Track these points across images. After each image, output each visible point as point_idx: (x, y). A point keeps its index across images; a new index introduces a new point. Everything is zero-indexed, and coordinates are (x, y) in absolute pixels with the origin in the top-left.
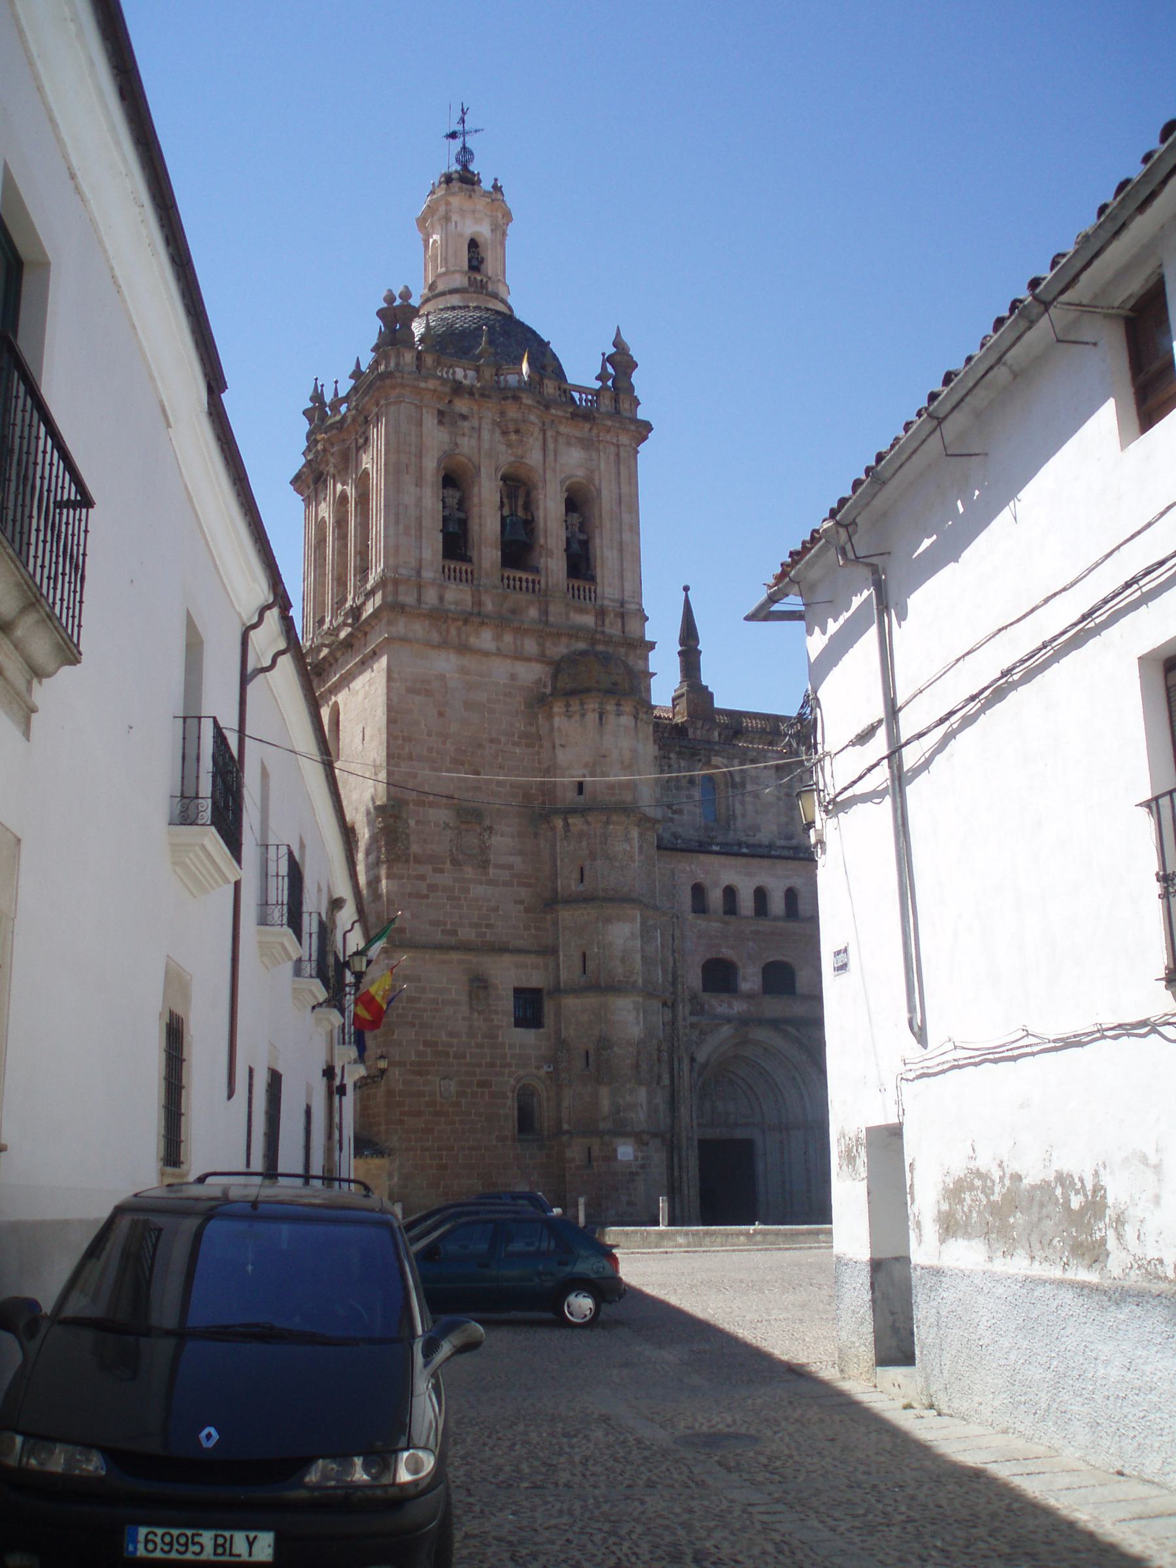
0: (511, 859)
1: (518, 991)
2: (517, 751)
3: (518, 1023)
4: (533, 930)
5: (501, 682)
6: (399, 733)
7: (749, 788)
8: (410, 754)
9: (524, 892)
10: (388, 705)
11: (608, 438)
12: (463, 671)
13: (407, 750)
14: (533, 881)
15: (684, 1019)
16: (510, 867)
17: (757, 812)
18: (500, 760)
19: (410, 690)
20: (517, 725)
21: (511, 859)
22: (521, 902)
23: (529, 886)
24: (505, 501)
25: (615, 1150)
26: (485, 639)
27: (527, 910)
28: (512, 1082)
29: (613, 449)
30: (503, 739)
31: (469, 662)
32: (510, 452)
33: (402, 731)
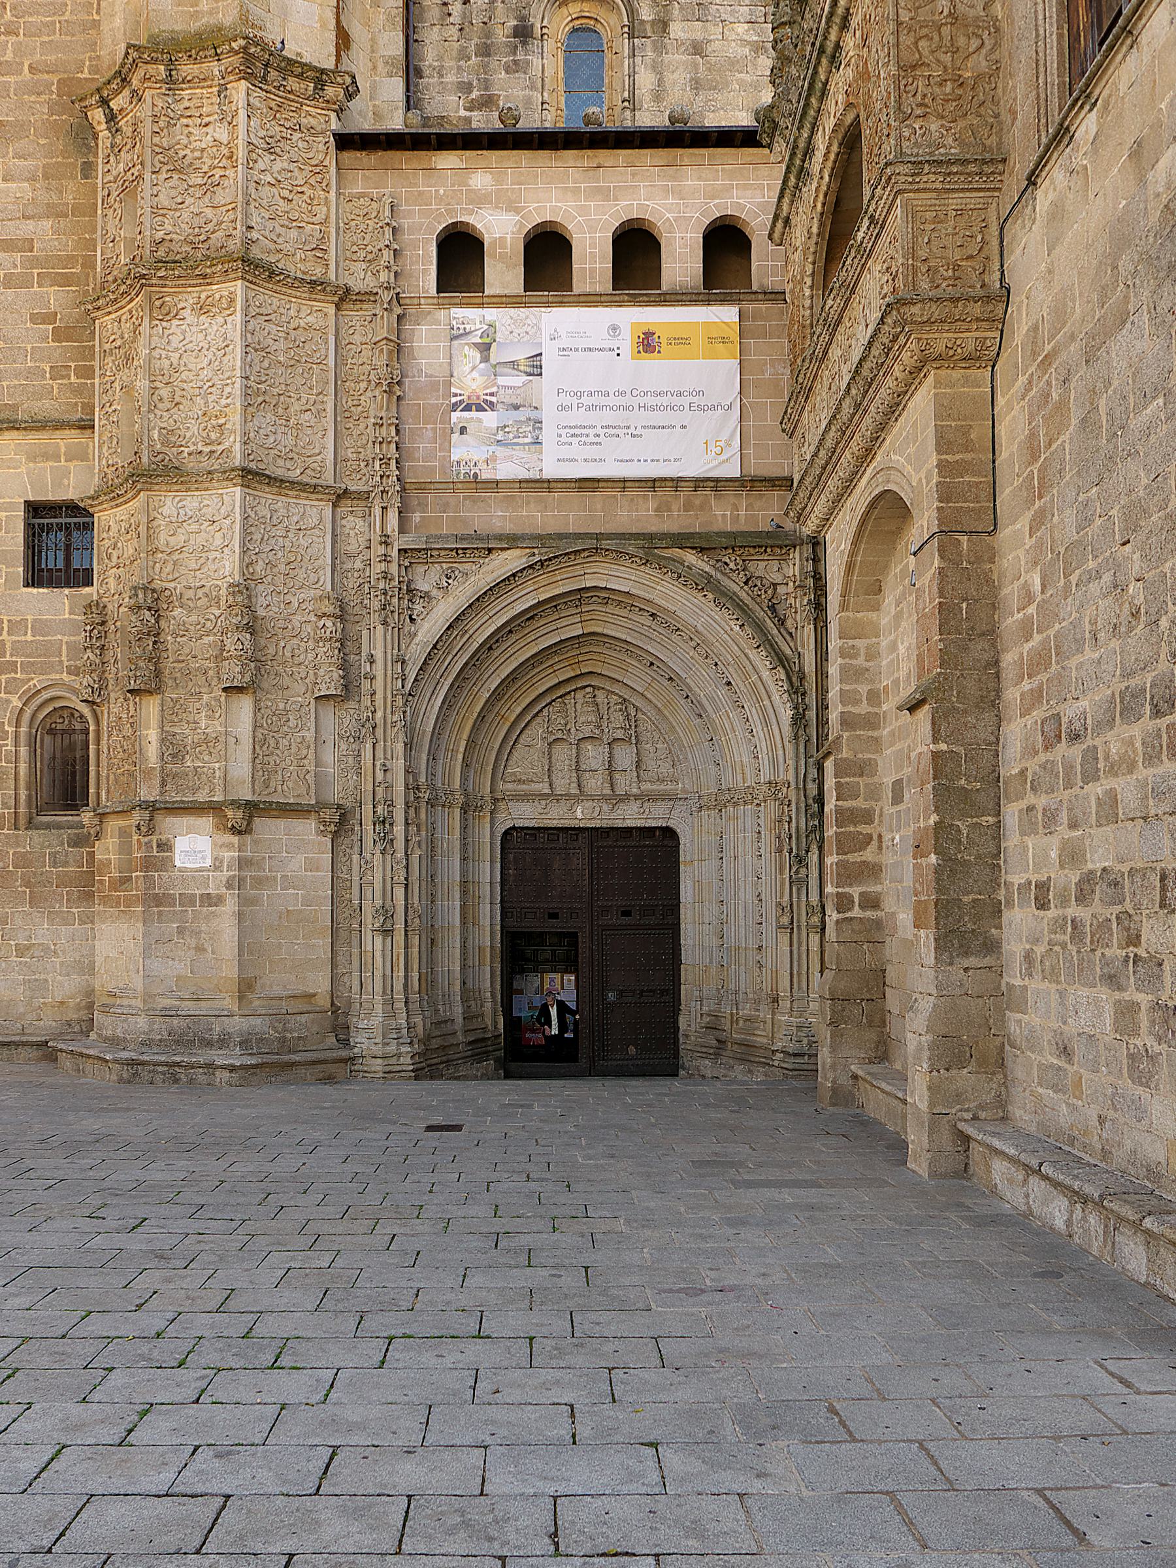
0: (28, 228)
1: (34, 509)
3: (37, 576)
4: (73, 379)
7: (677, 29)
9: (55, 297)
14: (77, 270)
15: (386, 541)
16: (29, 244)
17: (697, 85)
21: (28, 228)
22: (49, 318)
23: (66, 280)
25: (165, 846)
27: (58, 335)
28: (17, 703)
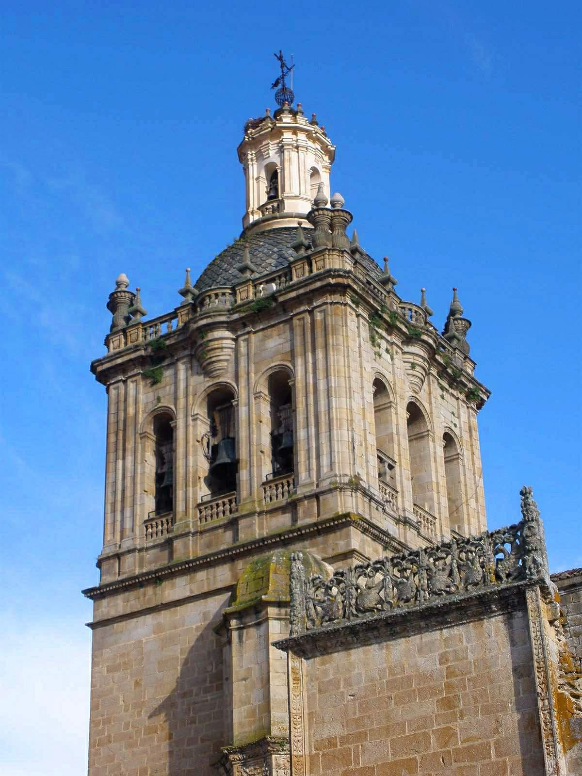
2: (209, 698)
5: (194, 627)
6: (100, 718)
8: (109, 736)
10: (92, 692)
11: (302, 308)
12: (158, 629)
13: (106, 734)
18: (191, 714)
19: (109, 671)
20: (209, 668)
24: (219, 428)
26: (178, 588)
29: (308, 318)
30: (195, 689)
31: (164, 617)
32: (207, 379)
33: (102, 715)
